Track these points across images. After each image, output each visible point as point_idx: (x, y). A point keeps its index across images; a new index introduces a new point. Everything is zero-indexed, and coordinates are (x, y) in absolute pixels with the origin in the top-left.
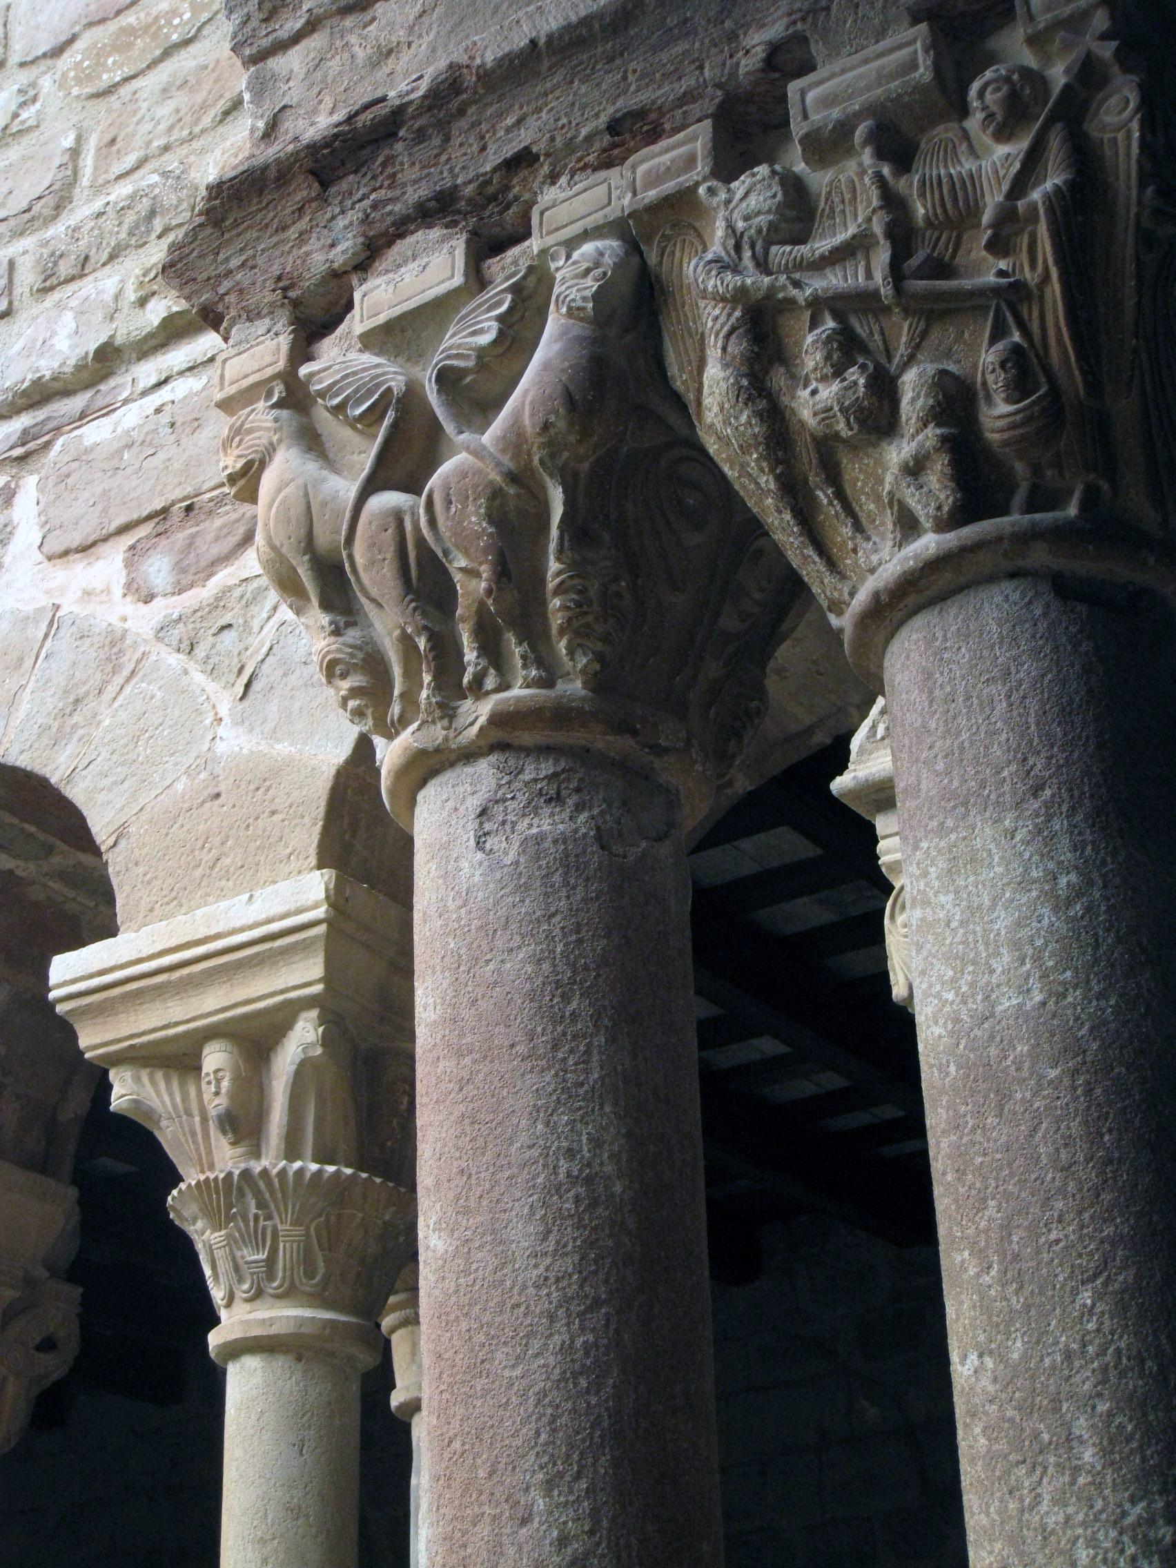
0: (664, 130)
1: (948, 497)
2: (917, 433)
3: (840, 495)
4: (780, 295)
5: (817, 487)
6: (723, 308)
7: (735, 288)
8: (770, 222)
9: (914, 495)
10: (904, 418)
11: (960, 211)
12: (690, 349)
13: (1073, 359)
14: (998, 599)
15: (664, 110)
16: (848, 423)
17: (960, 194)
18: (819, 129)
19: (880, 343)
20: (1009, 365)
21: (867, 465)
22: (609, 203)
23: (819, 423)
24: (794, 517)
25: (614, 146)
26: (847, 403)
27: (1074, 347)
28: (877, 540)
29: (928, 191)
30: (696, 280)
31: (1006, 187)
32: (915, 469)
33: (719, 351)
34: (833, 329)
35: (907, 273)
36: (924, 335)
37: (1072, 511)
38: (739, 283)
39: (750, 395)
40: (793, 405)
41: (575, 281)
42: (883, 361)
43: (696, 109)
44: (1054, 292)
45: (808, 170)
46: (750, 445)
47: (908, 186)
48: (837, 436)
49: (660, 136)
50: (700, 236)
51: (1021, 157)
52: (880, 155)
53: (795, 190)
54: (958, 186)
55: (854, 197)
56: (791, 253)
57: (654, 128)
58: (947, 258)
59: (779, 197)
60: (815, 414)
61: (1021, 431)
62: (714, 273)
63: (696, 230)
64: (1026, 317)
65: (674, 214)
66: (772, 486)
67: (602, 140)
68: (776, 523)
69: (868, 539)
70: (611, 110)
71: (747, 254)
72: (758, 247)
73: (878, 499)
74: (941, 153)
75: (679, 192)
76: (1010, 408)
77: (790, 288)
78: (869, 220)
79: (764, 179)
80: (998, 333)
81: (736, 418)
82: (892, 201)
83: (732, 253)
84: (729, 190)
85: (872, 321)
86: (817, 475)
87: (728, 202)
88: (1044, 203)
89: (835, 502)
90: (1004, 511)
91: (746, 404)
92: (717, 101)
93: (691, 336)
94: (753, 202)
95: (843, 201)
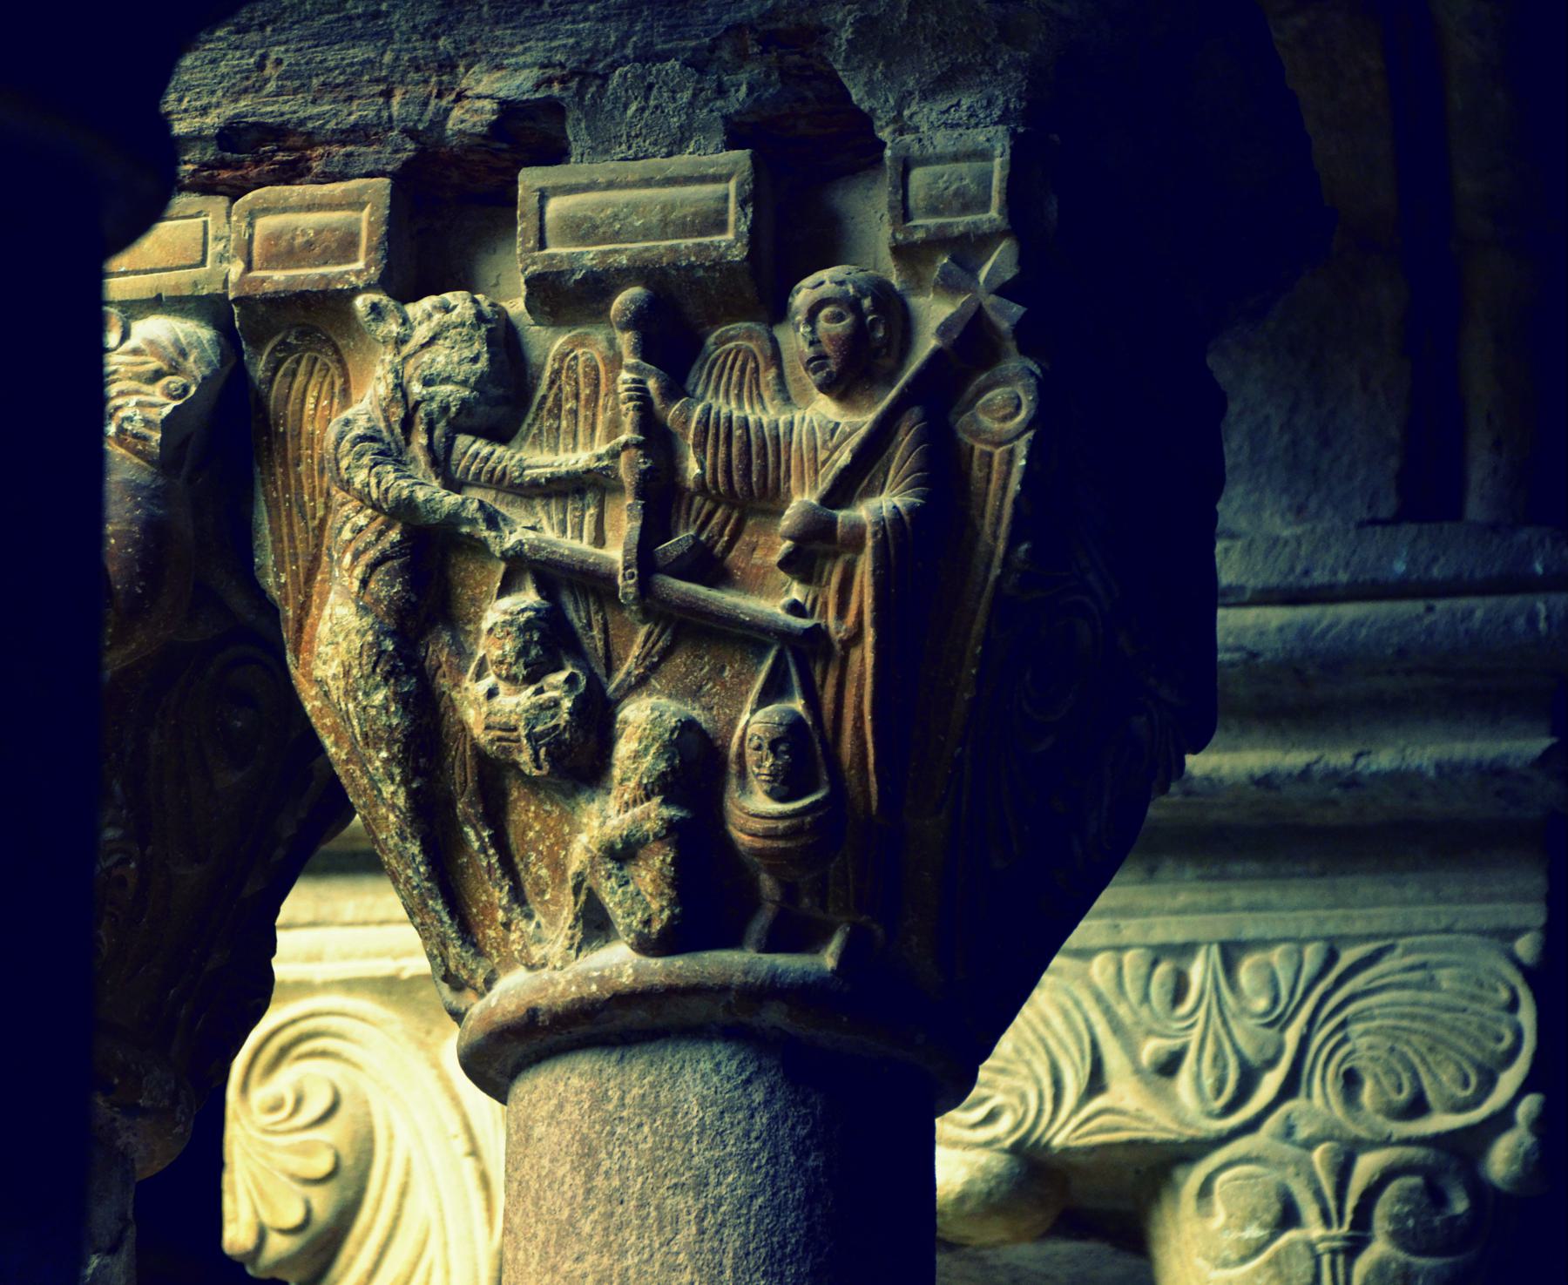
0: (309, 169)
1: (662, 909)
2: (635, 803)
3: (500, 841)
4: (465, 529)
5: (468, 821)
6: (373, 519)
7: (398, 500)
8: (464, 401)
9: (614, 893)
10: (617, 773)
11: (753, 481)
12: (299, 536)
13: (871, 759)
14: (706, 1066)
15: (317, 138)
16: (536, 759)
17: (756, 462)
18: (560, 274)
19: (600, 644)
20: (782, 748)
21: (549, 813)
22: (203, 263)
23: (492, 742)
24: (424, 851)
25: (223, 165)
26: (538, 729)
28: (543, 921)
29: (710, 441)
30: (337, 462)
31: (824, 485)
32: (623, 853)
33: (356, 584)
34: (537, 610)
35: (662, 563)
36: (666, 654)
37: (828, 959)
38: (405, 493)
39: (394, 667)
40: (454, 694)
41: (133, 385)
42: (600, 671)
43: (368, 154)
44: (863, 659)
45: (528, 319)
46: (381, 739)
48: (515, 765)
49: (301, 175)
50: (341, 361)
51: (855, 440)
52: (646, 350)
53: (503, 340)
54: (754, 449)
55: (596, 392)
56: (487, 459)
57: (295, 162)
58: (719, 547)
59: (482, 364)
60: (488, 728)
61: (781, 844)
62: (366, 460)
63: (337, 351)
64: (818, 679)
65: (309, 323)
66: (401, 801)
67: (204, 149)
68: (391, 842)
69: (529, 916)
70: (229, 110)
71: (420, 439)
73: (558, 867)
74: (736, 373)
75: (324, 292)
77: (483, 526)
78: (614, 455)
79: (463, 324)
80: (773, 691)
81: (366, 694)
82: (656, 438)
83: (398, 430)
84: (405, 321)
85: (593, 608)
86: (470, 804)
87: (401, 341)
88: (875, 534)
89: (491, 851)
90: (733, 941)
91: (386, 680)
92: (404, 156)
93: (304, 517)
94: (441, 358)
95: (577, 396)
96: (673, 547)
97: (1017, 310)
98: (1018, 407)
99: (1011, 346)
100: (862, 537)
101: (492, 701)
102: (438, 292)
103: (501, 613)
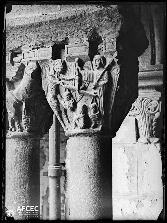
3: (67, 116)
27: (104, 107)
31: (97, 80)
37: (99, 129)
47: (81, 72)
53: (64, 64)
59: (62, 67)
72: (58, 74)
76: (93, 114)
87: (54, 65)
96: (81, 87)
97: (118, 60)
98: (118, 71)
99: (117, 64)
100: (101, 86)
101: (65, 103)
102: (58, 59)
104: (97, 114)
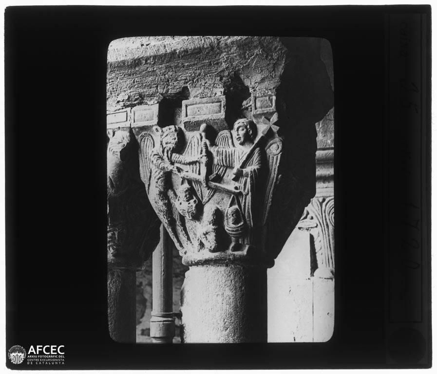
3: (185, 229)
12: (147, 172)
27: (252, 215)
31: (241, 164)
34: (188, 188)
37: (245, 252)
47: (213, 150)
53: (181, 135)
59: (176, 140)
71: (165, 154)
72: (169, 152)
76: (234, 226)
86: (179, 223)
87: (162, 136)
97: (278, 128)
98: (278, 148)
99: (277, 135)
100: (248, 174)
101: (182, 205)
103: (181, 189)
104: (241, 226)
